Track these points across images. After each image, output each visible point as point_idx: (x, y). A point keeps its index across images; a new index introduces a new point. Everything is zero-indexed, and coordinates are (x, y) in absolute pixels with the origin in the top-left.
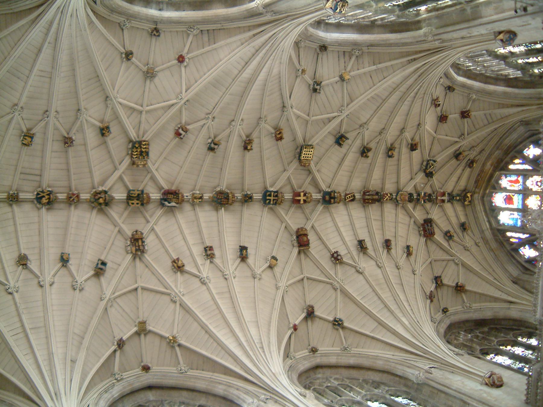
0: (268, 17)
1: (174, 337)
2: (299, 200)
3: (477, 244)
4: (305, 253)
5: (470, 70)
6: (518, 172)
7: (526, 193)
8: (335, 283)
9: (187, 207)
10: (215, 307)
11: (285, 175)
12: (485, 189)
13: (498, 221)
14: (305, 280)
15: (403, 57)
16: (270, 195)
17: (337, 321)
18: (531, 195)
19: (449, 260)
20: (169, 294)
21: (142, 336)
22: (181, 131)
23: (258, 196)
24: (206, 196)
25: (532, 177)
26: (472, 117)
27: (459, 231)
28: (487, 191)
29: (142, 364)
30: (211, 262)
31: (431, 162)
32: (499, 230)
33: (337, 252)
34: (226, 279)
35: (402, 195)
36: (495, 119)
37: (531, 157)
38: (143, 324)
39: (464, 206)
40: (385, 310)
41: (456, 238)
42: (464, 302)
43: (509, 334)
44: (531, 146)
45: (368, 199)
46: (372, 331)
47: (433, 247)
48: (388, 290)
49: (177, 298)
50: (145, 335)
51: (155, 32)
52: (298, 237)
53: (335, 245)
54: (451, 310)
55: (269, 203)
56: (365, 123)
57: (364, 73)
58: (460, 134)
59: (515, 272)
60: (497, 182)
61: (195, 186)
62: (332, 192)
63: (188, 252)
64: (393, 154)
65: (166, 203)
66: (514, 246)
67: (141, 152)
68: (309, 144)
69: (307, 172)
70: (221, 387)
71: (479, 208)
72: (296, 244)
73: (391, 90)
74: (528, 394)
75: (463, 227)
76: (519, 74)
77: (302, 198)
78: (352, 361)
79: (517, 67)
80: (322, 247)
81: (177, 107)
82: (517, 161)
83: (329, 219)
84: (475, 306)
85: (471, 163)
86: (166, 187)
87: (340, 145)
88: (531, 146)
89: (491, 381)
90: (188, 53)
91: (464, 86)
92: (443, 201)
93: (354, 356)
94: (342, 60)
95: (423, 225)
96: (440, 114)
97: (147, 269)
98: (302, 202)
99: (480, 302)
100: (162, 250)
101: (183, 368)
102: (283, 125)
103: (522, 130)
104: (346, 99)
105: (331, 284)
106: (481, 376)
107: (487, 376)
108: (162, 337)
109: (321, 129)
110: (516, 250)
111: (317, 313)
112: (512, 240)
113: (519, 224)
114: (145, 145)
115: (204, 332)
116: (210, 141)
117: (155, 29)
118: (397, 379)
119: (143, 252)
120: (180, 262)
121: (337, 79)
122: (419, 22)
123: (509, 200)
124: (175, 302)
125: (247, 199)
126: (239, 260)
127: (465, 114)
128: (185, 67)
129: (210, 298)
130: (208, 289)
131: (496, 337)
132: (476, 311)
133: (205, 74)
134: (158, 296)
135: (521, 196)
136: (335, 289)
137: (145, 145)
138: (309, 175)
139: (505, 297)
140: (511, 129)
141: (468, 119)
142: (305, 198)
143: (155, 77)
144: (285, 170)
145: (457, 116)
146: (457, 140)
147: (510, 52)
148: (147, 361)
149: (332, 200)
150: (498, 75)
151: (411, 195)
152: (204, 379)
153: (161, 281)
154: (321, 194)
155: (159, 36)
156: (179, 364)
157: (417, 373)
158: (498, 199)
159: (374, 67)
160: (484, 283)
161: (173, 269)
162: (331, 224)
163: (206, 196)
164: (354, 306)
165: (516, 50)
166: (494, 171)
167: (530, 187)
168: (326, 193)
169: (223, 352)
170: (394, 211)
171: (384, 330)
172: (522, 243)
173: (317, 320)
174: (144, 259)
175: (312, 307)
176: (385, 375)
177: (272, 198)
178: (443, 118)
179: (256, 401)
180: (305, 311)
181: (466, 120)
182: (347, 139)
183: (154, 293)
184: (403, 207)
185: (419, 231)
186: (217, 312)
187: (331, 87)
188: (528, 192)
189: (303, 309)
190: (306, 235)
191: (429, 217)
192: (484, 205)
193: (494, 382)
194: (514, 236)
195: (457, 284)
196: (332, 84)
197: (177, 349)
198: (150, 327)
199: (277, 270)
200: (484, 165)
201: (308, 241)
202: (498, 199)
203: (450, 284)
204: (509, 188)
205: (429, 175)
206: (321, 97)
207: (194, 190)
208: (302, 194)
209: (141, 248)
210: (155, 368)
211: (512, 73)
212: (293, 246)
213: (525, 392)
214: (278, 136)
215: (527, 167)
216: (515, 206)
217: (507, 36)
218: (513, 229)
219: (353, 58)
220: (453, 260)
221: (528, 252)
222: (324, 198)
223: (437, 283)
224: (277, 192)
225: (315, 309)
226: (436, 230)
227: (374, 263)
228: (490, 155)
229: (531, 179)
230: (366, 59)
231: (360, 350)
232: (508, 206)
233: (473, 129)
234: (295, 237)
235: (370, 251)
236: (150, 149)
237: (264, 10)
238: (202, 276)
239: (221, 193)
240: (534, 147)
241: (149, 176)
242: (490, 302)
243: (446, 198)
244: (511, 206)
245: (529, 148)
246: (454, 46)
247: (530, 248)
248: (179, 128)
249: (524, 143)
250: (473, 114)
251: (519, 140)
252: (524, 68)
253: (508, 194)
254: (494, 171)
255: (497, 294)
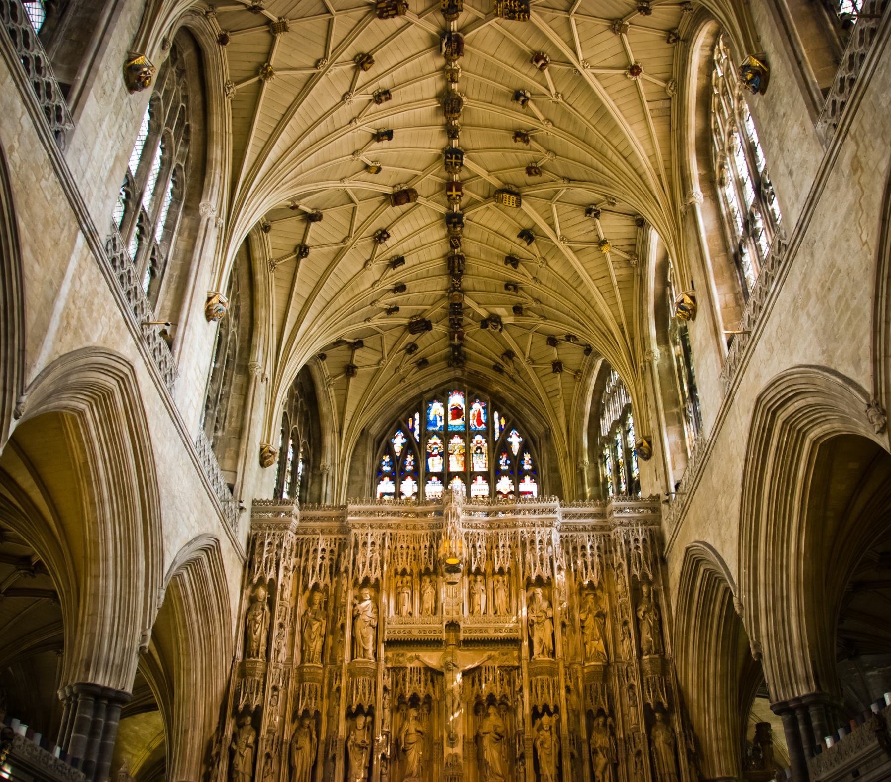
0: (680, 208)
1: (271, 73)
2: (452, 191)
3: (402, 379)
4: (384, 201)
5: (610, 375)
6: (490, 423)
7: (467, 434)
8: (351, 241)
9: (441, 62)
10: (315, 118)
11: (483, 173)
12: (467, 383)
13: (432, 402)
14: (353, 205)
15: (626, 318)
16: (457, 158)
17: (305, 250)
18: (465, 441)
19: (382, 352)
20: (325, 57)
21: (266, 28)
22: (542, 62)
23: (455, 143)
24: (455, 86)
25: (486, 442)
26: (555, 375)
27: (417, 357)
28: (465, 385)
29: (228, 34)
30: (370, 101)
31: (500, 327)
32: (421, 403)
33: (388, 236)
34: (351, 122)
35: (460, 296)
36: (553, 400)
37: (510, 440)
38: (285, 29)
39: (446, 358)
40: (324, 304)
41: (408, 357)
42: (335, 377)
43: (304, 437)
44: (521, 440)
45: (454, 263)
46: (298, 294)
47: (397, 333)
48: (347, 300)
49: (322, 70)
50: (268, 31)
51: (673, 38)
52: (405, 191)
53: (396, 234)
54: (324, 364)
55: (447, 158)
56: (547, 265)
57: (608, 270)
58: (534, 358)
59: (374, 431)
60: (477, 397)
61: (467, 71)
62: (463, 223)
63: (382, 70)
64: (510, 289)
65: (446, 41)
66: (405, 425)
67: (514, 12)
68: (523, 201)
69: (486, 195)
70: (219, 152)
71: (445, 377)
72: (397, 189)
73: (588, 299)
74: (264, 502)
75: (423, 363)
76: (605, 432)
77: (454, 193)
78: (260, 277)
79: (612, 432)
80: (394, 217)
81: (572, 59)
82: (503, 422)
83: (428, 221)
84: (332, 391)
85: (498, 369)
86: (467, 37)
87: (521, 236)
88: (521, 440)
89: (266, 455)
90: (642, 79)
91: (591, 367)
92: (452, 338)
93: (267, 279)
94: (625, 243)
95: (423, 320)
96: (557, 337)
97: (356, 22)
98: (449, 193)
99: (336, 396)
100: (382, 38)
101: (231, 91)
102: (546, 175)
103: (541, 430)
104: (578, 246)
105: (349, 236)
106: (268, 442)
107: (272, 449)
108: (269, 54)
109: (541, 215)
110: (399, 428)
111: (313, 225)
112: (410, 423)
113: (431, 428)
114: (524, 17)
115: (283, 112)
116: (528, 95)
117: (678, 38)
118: (247, 337)
119: (381, 17)
120: (368, 66)
121: (603, 237)
122: (667, 343)
123: (457, 413)
124: (316, 66)
125: (452, 132)
126: (375, 132)
127: (557, 366)
128: (625, 75)
129: (326, 111)
130: (336, 106)
131: (300, 423)
132: (326, 393)
133: (614, 101)
134: (323, 42)
135: (462, 429)
136: (343, 241)
137: (524, 17)
138: (482, 197)
139: (346, 424)
140: (540, 417)
141: (552, 370)
142: (454, 196)
143: (615, 33)
144: (489, 172)
145: (556, 357)
146: (527, 356)
147: (629, 430)
148: (233, 38)
149: (452, 225)
150: (604, 405)
151: (460, 304)
152: (223, 125)
153: (343, 43)
154: (459, 212)
155: (668, 42)
156: (237, 83)
157: (260, 365)
158: (457, 400)
159: (615, 283)
160: (359, 398)
161: (358, 55)
162: (422, 224)
163: (455, 86)
164: (324, 266)
165: (631, 438)
166: (490, 394)
167: (474, 441)
168: (460, 217)
169: (262, 144)
170: (439, 288)
171: (300, 308)
172: (409, 434)
173: (304, 226)
174: (369, 17)
175: (320, 220)
176: (248, 320)
177: (454, 161)
178: (552, 341)
179: (215, 213)
180: (315, 212)
181: (551, 366)
182: (529, 244)
183: (324, 35)
184: (443, 296)
185: (415, 316)
186: (310, 123)
187: (592, 228)
188: (468, 438)
189: (316, 209)
190: (409, 201)
191: (433, 325)
192: (449, 381)
193: (266, 458)
194: (416, 421)
195: (357, 367)
196: (595, 229)
197: (256, 79)
198: (280, 37)
199: (364, 175)
200: (498, 382)
201: (402, 204)
202: (457, 400)
203: (355, 358)
204: (471, 412)
205: (484, 323)
206: (580, 217)
207: (463, 69)
208: (459, 193)
209: (385, 14)
210: (225, 49)
211: (606, 425)
212: (394, 186)
213: (265, 499)
214: (533, 171)
215: (497, 435)
216: (451, 422)
217: (646, 451)
218: (425, 422)
219: (626, 257)
220: (383, 358)
221: (399, 442)
222: (455, 215)
223: (355, 344)
224: (462, 165)
225: (318, 222)
226: (418, 334)
227: (377, 278)
228: (510, 390)
229: (483, 440)
230: (624, 272)
231: (273, 282)
232: (450, 412)
233: (540, 374)
234: (405, 188)
235: (391, 271)
236: (518, 23)
237: (688, 204)
238: (352, 95)
239: (460, 102)
240: (520, 443)
241: (481, 16)
242: (338, 408)
243: (456, 342)
244: (450, 417)
245: (519, 437)
246: (637, 383)
247: (403, 444)
248: (545, 59)
249: (525, 431)
250: (559, 376)
251: (528, 425)
252: (610, 439)
253: (464, 411)
254: (490, 394)
255: (348, 416)
